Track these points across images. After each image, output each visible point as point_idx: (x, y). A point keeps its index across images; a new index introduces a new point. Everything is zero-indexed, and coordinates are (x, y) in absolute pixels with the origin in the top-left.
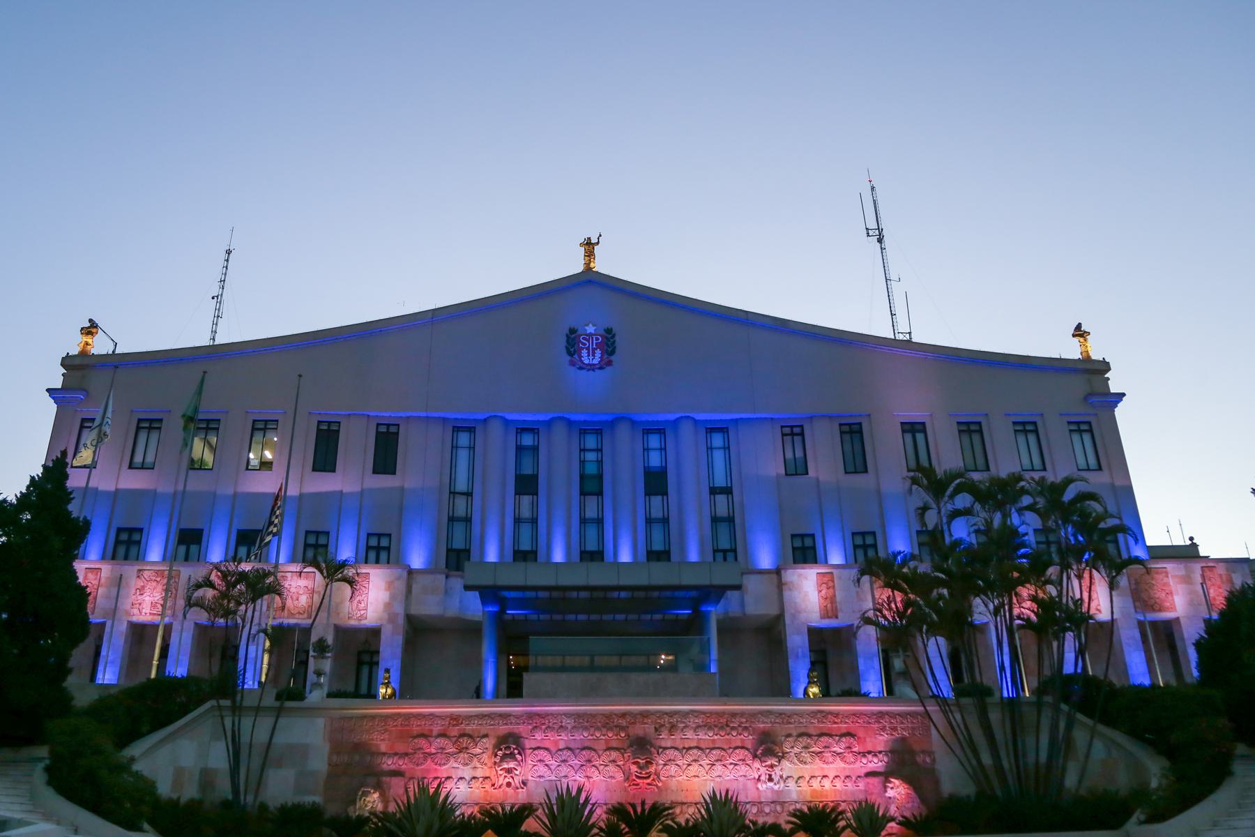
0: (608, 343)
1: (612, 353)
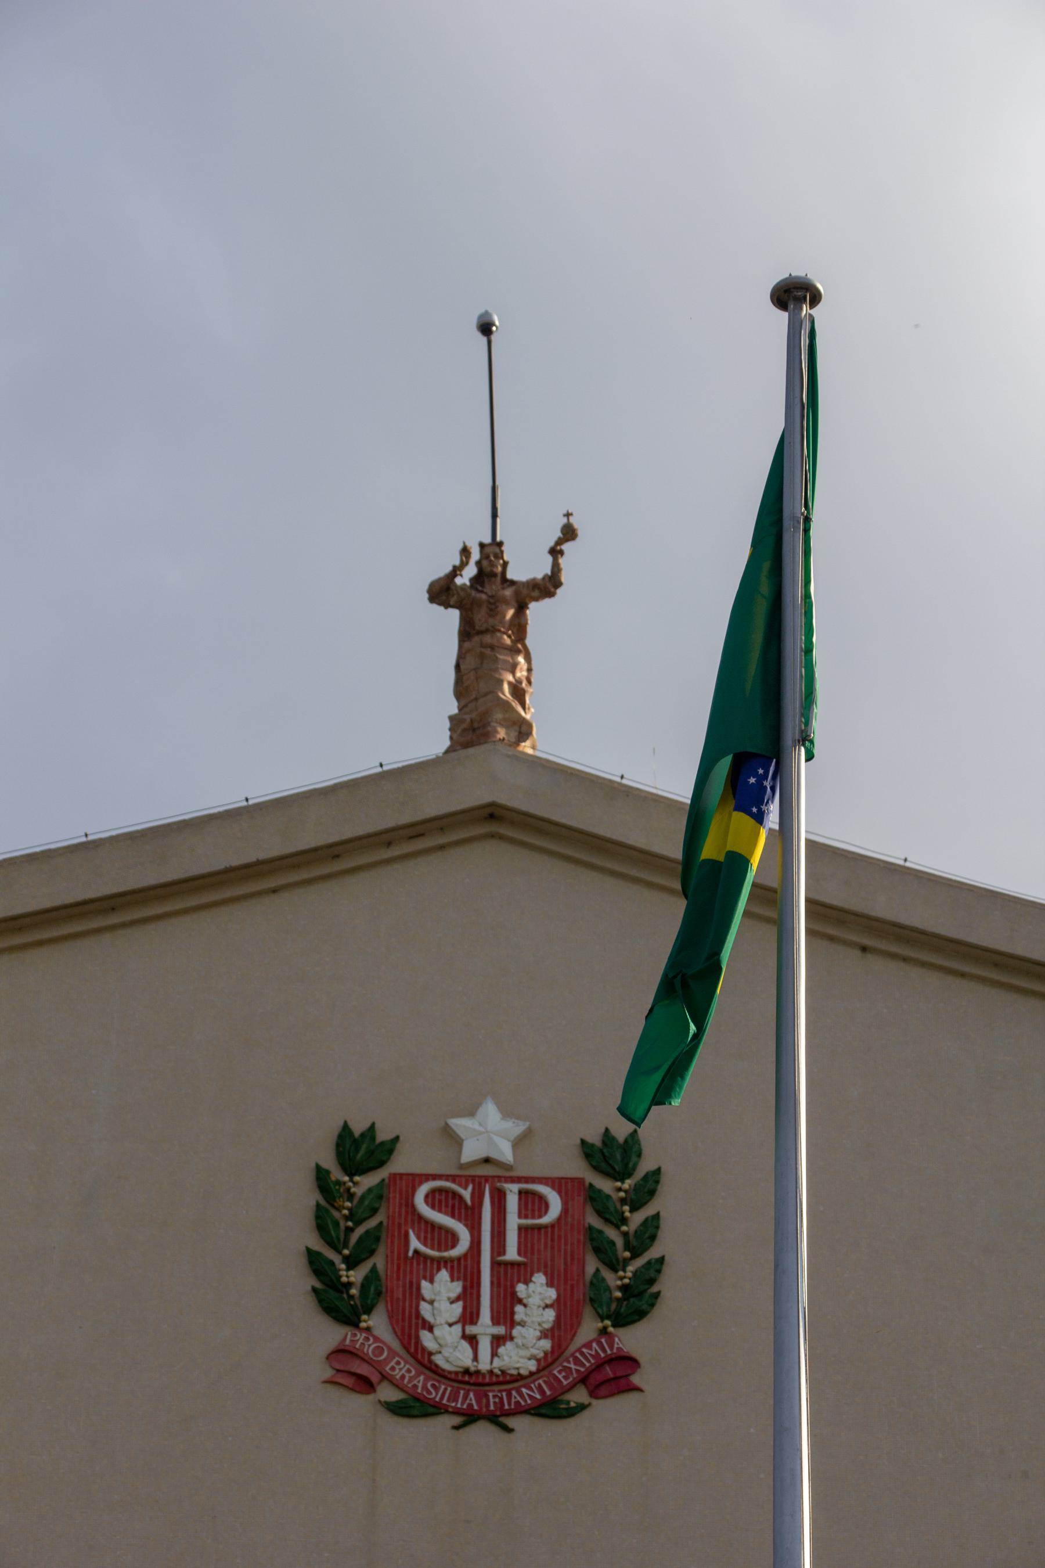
1: (636, 1303)
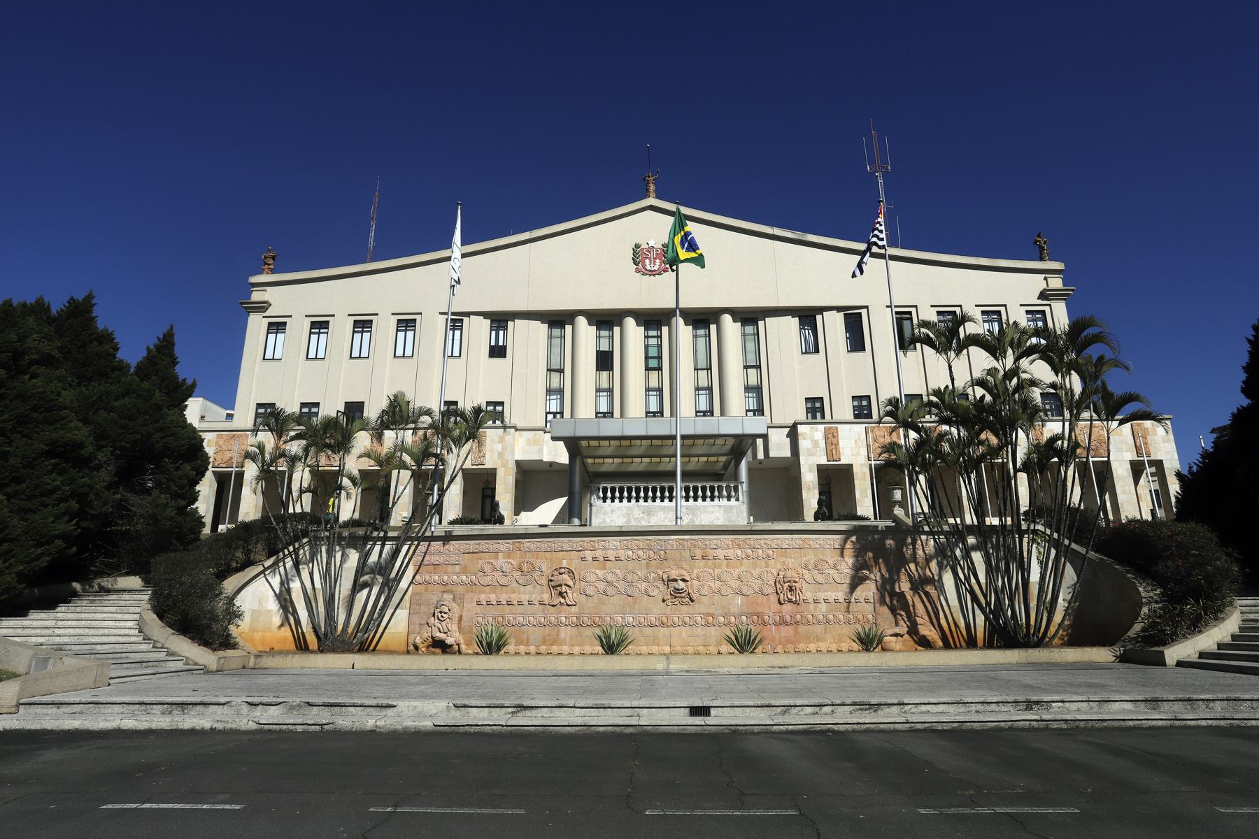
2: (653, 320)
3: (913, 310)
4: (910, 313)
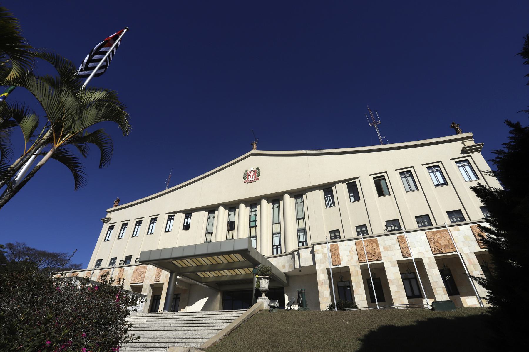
0: (257, 172)
2: (253, 203)
3: (385, 174)
4: (384, 176)
